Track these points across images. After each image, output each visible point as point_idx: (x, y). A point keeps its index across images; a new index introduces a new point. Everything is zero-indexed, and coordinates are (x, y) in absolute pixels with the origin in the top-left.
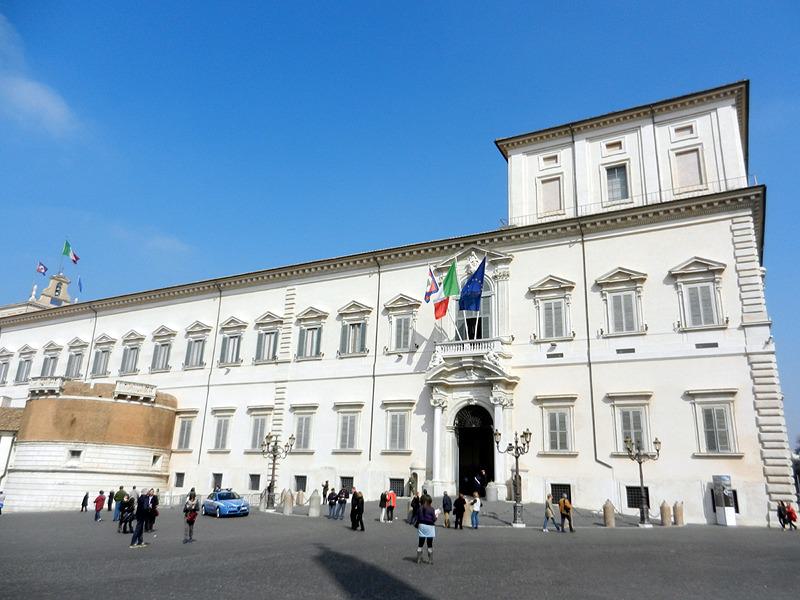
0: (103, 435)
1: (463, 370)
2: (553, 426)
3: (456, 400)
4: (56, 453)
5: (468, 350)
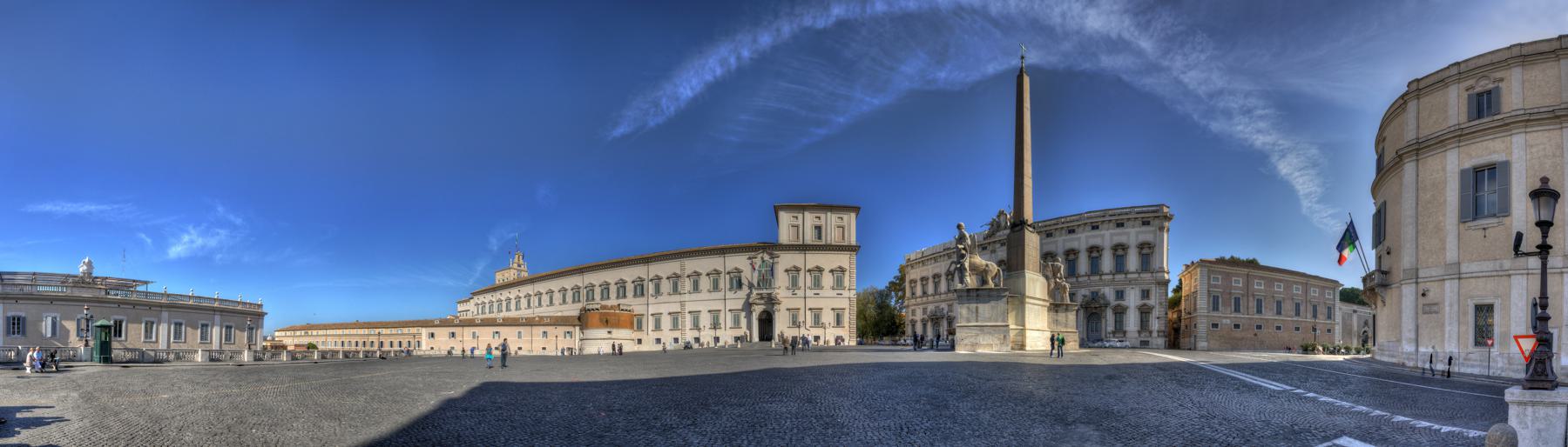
0: (618, 325)
1: (762, 298)
2: (793, 318)
3: (758, 310)
4: (602, 333)
5: (765, 291)
